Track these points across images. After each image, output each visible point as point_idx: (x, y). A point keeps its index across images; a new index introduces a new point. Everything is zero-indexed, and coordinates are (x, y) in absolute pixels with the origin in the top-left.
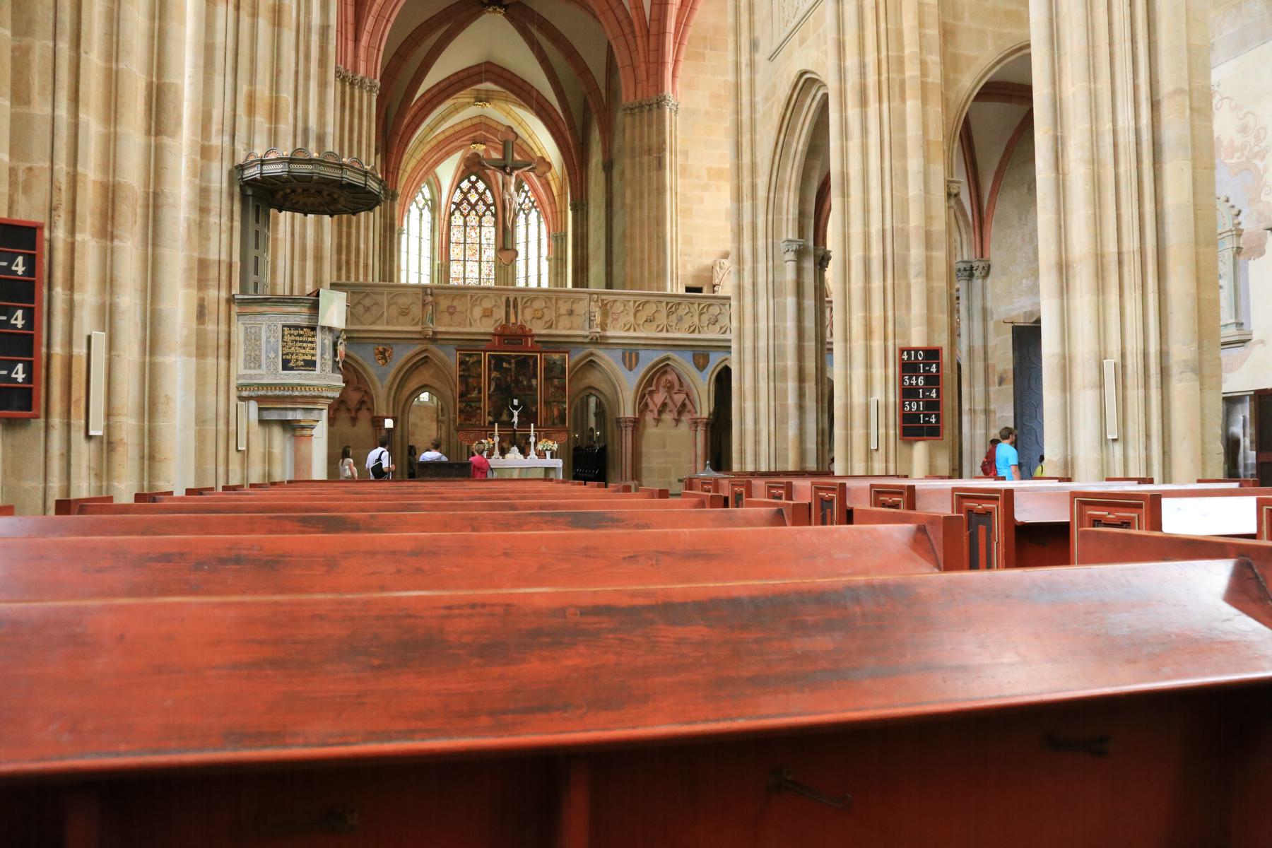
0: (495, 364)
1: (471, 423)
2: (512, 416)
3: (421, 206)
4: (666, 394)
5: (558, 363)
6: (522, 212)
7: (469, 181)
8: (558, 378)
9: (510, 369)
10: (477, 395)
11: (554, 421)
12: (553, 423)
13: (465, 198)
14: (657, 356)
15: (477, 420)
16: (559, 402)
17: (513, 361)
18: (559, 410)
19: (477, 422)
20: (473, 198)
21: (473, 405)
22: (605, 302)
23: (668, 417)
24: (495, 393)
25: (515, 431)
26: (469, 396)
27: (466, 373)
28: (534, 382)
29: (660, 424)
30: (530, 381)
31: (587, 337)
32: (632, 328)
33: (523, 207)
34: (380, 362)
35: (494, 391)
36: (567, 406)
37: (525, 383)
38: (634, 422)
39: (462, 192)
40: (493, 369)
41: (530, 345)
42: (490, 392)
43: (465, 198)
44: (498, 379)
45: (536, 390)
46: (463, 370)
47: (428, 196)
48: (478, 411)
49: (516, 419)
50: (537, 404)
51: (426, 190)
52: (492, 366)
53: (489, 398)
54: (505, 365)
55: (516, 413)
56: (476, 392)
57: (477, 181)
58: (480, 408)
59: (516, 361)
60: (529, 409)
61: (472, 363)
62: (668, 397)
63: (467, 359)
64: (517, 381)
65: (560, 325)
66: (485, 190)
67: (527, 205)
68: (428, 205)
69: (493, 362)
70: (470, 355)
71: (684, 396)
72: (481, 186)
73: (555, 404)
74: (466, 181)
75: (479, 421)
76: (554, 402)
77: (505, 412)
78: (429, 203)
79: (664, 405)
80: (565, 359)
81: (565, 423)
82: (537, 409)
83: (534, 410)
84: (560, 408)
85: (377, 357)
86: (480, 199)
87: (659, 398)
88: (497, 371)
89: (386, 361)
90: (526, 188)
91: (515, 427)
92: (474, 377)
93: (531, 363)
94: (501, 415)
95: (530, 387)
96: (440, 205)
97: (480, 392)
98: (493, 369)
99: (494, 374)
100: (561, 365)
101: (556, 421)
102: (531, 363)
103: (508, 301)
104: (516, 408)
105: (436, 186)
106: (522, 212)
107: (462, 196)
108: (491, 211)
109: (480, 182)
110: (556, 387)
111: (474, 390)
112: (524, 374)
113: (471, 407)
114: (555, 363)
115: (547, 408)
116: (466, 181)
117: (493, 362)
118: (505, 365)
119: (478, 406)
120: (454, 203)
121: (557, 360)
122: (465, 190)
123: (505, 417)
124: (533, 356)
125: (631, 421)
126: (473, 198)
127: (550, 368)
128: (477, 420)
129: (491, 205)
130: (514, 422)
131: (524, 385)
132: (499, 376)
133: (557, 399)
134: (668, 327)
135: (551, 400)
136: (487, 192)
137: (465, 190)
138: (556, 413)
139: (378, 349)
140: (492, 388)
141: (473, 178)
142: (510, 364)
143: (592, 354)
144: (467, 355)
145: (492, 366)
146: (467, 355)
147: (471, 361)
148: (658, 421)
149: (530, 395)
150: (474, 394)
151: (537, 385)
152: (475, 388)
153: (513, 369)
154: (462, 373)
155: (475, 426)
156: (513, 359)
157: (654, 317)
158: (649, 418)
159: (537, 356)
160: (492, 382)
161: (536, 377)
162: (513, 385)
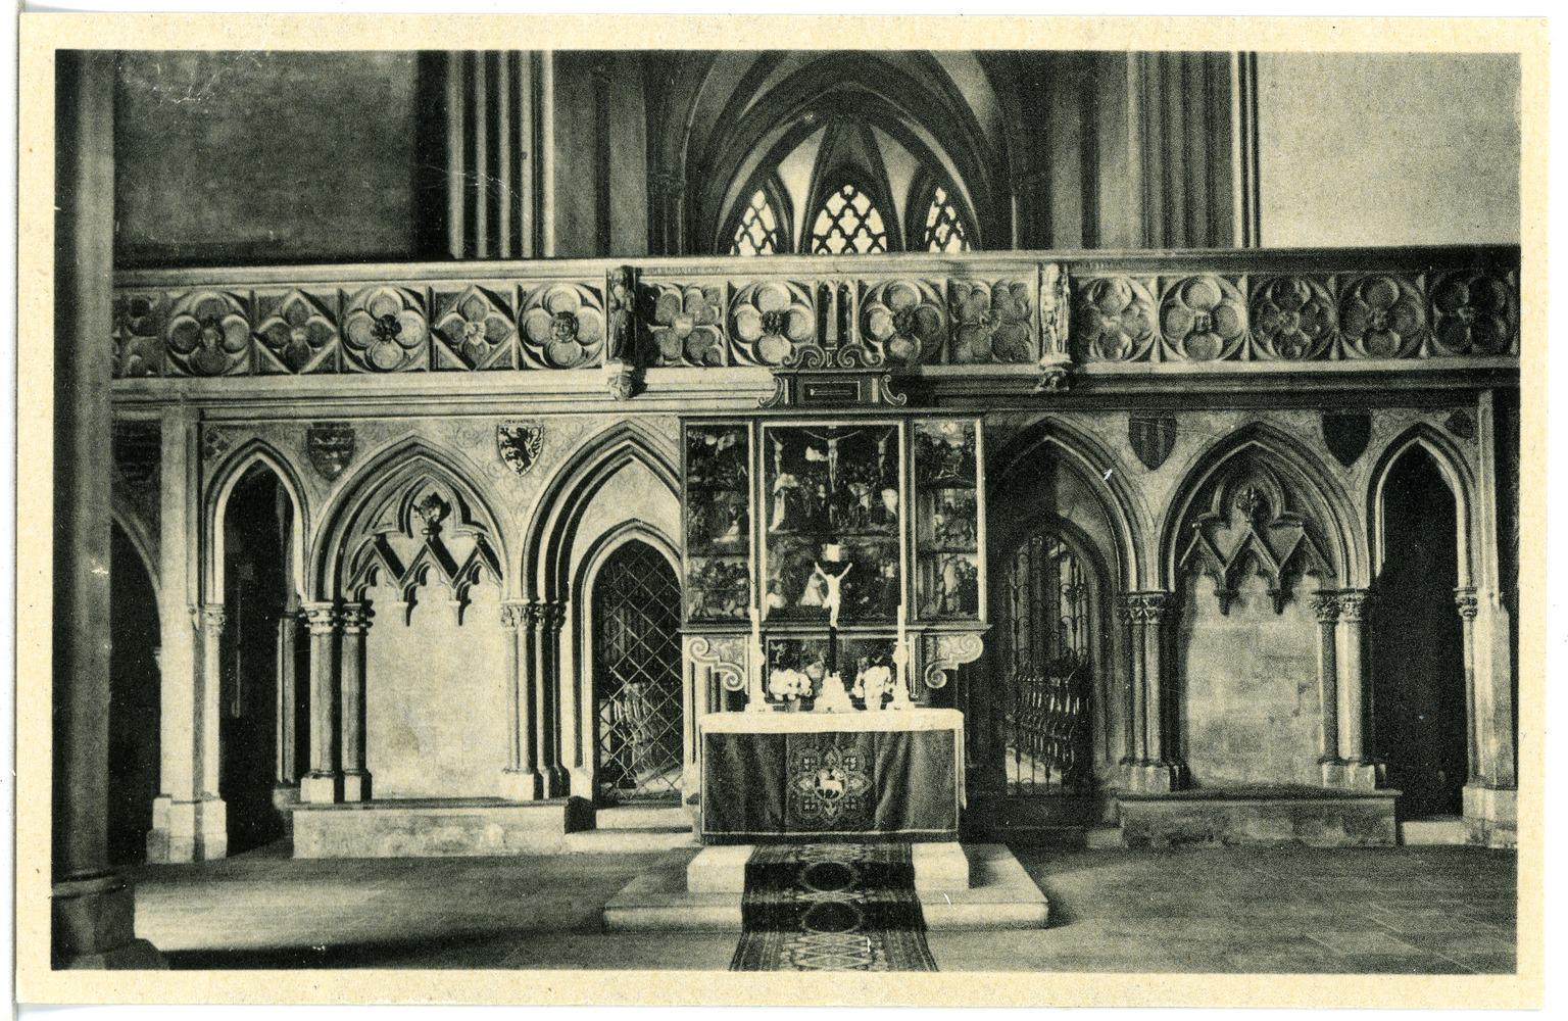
0: (782, 452)
1: (719, 611)
2: (824, 590)
3: (759, 243)
4: (1249, 528)
5: (954, 444)
6: (933, 243)
7: (844, 196)
8: (953, 485)
9: (824, 466)
10: (734, 539)
11: (944, 604)
12: (943, 609)
13: (836, 226)
14: (1224, 423)
15: (737, 606)
16: (964, 552)
17: (832, 443)
18: (959, 573)
19: (739, 612)
20: (849, 223)
21: (727, 562)
22: (1082, 283)
23: (1256, 588)
24: (786, 531)
25: (833, 632)
26: (716, 540)
27: (708, 479)
28: (889, 498)
29: (1233, 609)
30: (878, 496)
31: (1035, 380)
32: (1155, 351)
33: (937, 234)
34: (512, 464)
35: (781, 527)
36: (979, 561)
37: (865, 502)
38: (1165, 605)
39: (830, 216)
40: (778, 468)
41: (875, 399)
42: (772, 529)
43: (836, 226)
44: (792, 492)
45: (895, 520)
46: (700, 472)
47: (771, 225)
48: (741, 582)
49: (833, 601)
50: (898, 559)
51: (768, 216)
52: (777, 458)
53: (769, 546)
54: (812, 455)
55: (834, 582)
56: (735, 529)
57: (854, 195)
58: (746, 574)
59: (838, 448)
60: (877, 572)
61: (721, 453)
62: (1255, 534)
63: (711, 441)
64: (844, 498)
65: (964, 353)
66: (869, 210)
67: (944, 229)
68: (771, 242)
69: (779, 447)
70: (718, 431)
71: (1300, 531)
72: (862, 202)
73: (947, 556)
74: (838, 195)
75: (747, 605)
76: (946, 550)
77: (813, 582)
78: (774, 237)
79: (1244, 556)
80: (974, 434)
81: (975, 608)
82: (897, 572)
83: (890, 572)
84: (962, 566)
85: (504, 452)
86: (862, 225)
87: (1229, 539)
88: (788, 473)
89: (527, 463)
90: (941, 195)
91: (833, 623)
92: (725, 488)
93: (881, 444)
94: (802, 592)
95: (879, 513)
96: (792, 243)
97: (744, 530)
98: (778, 468)
99: (782, 480)
100: (963, 449)
101: (950, 601)
102: (881, 444)
103: (824, 291)
104: (833, 568)
105: (781, 202)
106: (933, 243)
107: (830, 222)
108: (880, 246)
109: (860, 195)
110: (948, 509)
111: (731, 525)
112: (862, 479)
113: (721, 568)
114: (944, 444)
115: (926, 568)
116: (838, 195)
117: (779, 447)
118: (812, 455)
119: (739, 567)
120: (818, 237)
121: (951, 437)
122: (835, 213)
123: (811, 597)
124: (888, 427)
125: (1153, 602)
126: (849, 223)
127: (931, 456)
128: (737, 606)
129: (880, 235)
130: (830, 609)
131: (862, 508)
132: (795, 484)
133: (952, 544)
134: (1256, 346)
135: (938, 547)
136: (874, 212)
137: (835, 213)
138: (950, 582)
139: (506, 434)
140: (779, 515)
141: (848, 189)
142: (824, 450)
143: (1049, 427)
144: (708, 430)
145: (777, 458)
146: (708, 430)
147: (721, 448)
148: (1229, 597)
149: (878, 533)
150: (731, 536)
151: (897, 508)
152: (732, 518)
153: (833, 466)
154: (697, 479)
155: (734, 621)
156: (831, 438)
157: (1215, 322)
158: (1205, 589)
159: (897, 427)
160: (777, 499)
161: (895, 486)
162: (832, 508)
